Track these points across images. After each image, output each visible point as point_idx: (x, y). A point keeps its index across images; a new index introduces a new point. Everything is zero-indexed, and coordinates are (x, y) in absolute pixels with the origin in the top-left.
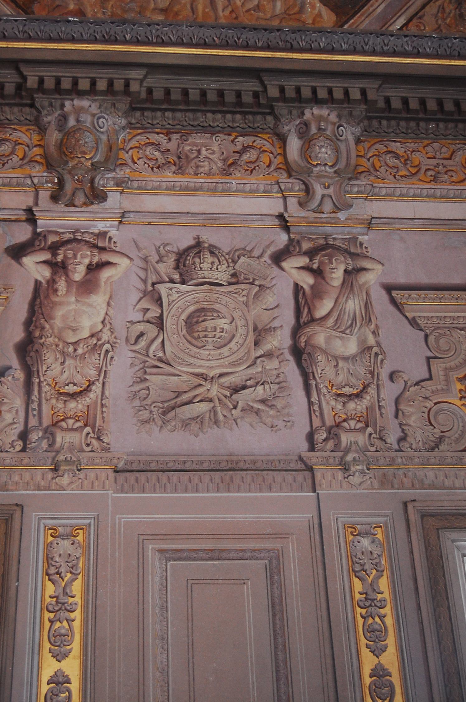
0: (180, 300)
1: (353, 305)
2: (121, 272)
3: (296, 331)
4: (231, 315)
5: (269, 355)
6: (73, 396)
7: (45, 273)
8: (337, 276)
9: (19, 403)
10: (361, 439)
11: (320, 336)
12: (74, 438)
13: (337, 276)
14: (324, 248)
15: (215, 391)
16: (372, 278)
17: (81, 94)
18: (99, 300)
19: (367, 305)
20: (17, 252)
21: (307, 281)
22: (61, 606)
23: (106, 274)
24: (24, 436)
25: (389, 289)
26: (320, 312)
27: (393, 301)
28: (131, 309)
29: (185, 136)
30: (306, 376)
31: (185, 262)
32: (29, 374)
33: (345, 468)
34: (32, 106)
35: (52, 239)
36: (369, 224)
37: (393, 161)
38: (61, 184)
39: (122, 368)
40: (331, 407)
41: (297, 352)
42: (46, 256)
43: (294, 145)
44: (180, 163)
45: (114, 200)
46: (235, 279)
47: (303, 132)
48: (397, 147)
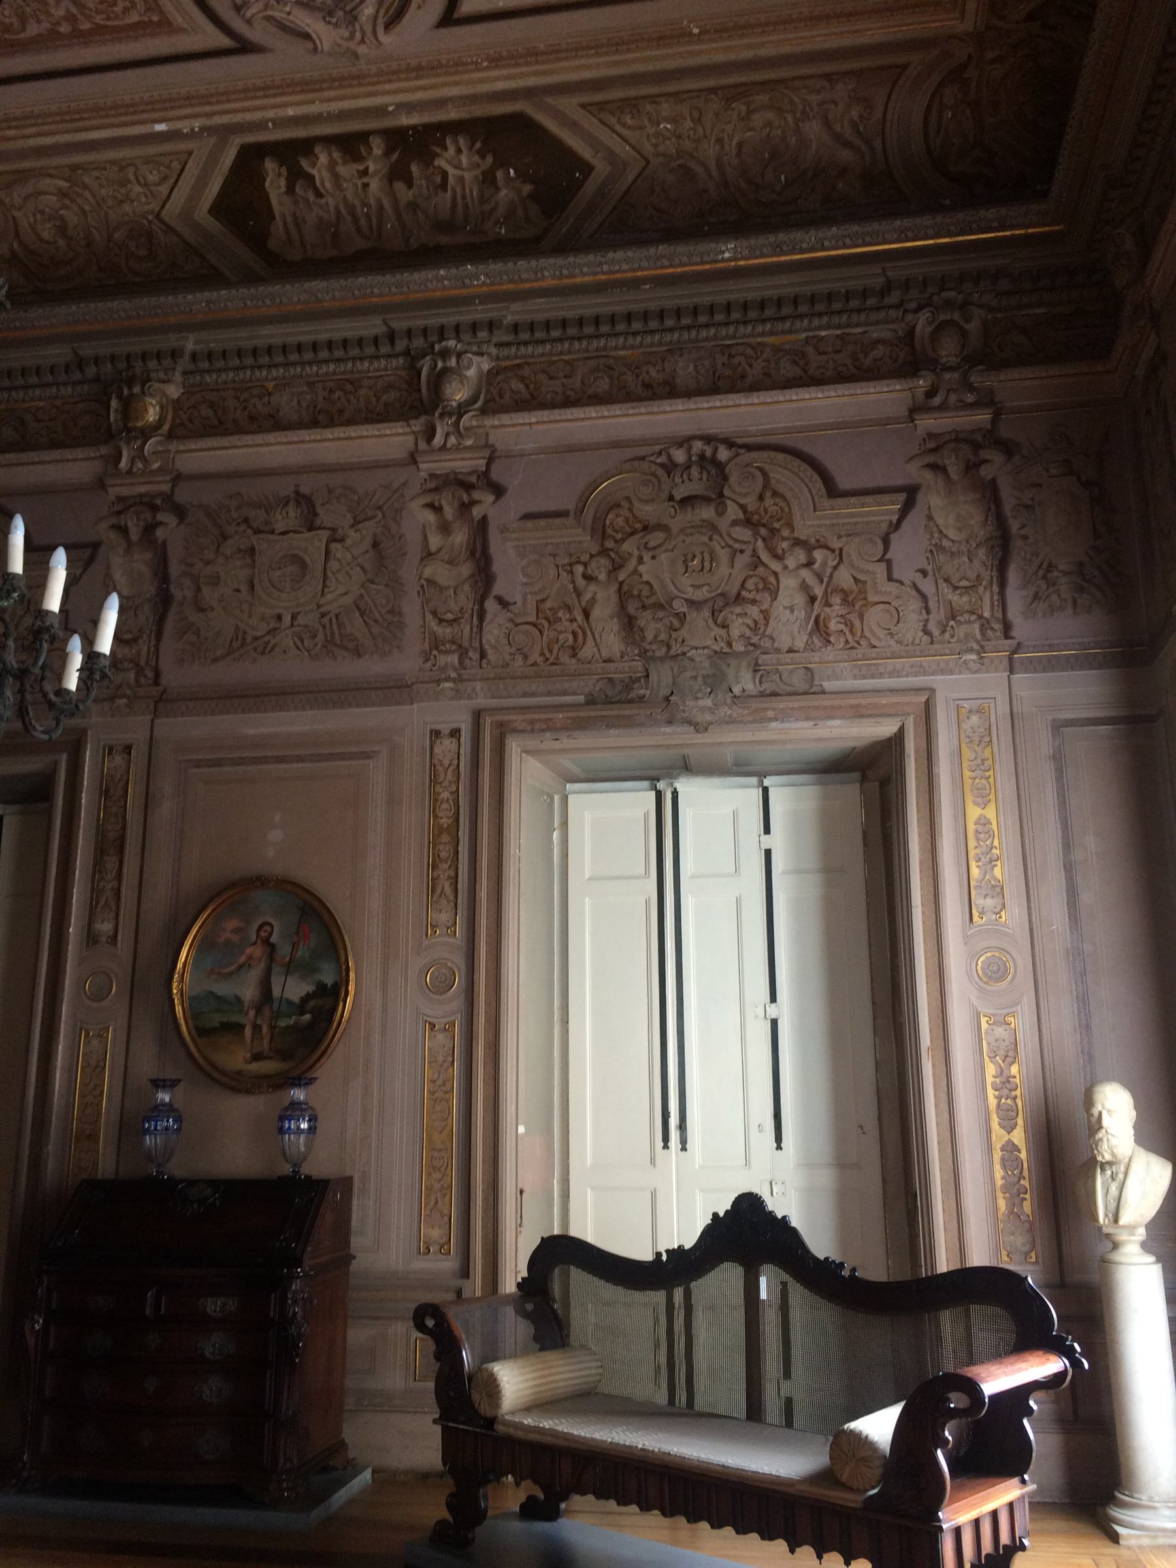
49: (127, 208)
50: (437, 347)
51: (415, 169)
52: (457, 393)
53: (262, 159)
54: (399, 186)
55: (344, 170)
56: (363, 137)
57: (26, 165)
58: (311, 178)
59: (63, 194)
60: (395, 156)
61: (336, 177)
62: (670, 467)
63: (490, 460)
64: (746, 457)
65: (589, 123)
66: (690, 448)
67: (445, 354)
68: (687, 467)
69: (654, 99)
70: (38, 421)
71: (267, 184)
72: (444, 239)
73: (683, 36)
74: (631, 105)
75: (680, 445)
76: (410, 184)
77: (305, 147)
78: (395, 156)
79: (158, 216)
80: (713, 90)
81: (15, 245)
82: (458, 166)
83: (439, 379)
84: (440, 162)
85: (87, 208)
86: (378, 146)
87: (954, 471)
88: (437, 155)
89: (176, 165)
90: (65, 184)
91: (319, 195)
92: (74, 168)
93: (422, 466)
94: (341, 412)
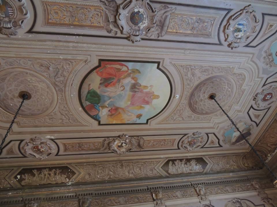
49: (150, 167)
50: (198, 186)
51: (188, 163)
52: (202, 193)
53: (170, 161)
54: (186, 165)
55: (179, 163)
56: (183, 159)
57: (139, 161)
58: (175, 164)
59: (142, 164)
60: (186, 161)
61: (178, 164)
62: (234, 202)
63: (210, 202)
64: (242, 201)
65: (209, 159)
66: (235, 200)
67: (200, 187)
68: (236, 202)
69: (216, 157)
70: (140, 198)
71: (169, 164)
72: (191, 172)
73: (223, 150)
74: (213, 157)
75: (233, 199)
76: (187, 165)
77: (176, 160)
78: (186, 161)
79: (154, 168)
80: (222, 156)
81: (133, 171)
82: (193, 163)
83: (200, 191)
84: (191, 162)
85: (145, 166)
86: (184, 160)
87: (267, 202)
88: (191, 162)
89: (159, 162)
90: (143, 163)
91: (175, 166)
92: (145, 162)
93: (201, 203)
94: (186, 195)
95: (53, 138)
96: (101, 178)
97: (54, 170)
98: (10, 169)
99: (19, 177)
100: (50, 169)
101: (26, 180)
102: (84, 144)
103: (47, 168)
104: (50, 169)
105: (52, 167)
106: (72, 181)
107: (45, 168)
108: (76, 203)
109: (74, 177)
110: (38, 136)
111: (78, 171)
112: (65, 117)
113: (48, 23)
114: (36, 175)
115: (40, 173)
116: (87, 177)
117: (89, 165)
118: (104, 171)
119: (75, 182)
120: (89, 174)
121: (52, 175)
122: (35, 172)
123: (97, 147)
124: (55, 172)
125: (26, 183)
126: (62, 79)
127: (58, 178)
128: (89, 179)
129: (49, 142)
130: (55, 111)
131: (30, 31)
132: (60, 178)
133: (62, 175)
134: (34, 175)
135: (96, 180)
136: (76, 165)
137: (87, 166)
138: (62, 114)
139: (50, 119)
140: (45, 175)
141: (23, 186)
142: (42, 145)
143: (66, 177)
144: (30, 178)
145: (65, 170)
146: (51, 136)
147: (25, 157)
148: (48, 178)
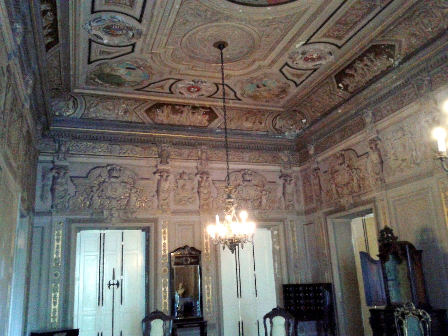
0: (181, 182)
1: (207, 184)
2: (171, 177)
3: (198, 188)
4: (188, 186)
5: (194, 193)
6: (165, 200)
7: (159, 177)
8: (205, 179)
9: (157, 201)
10: (206, 207)
11: (202, 189)
12: (165, 207)
13: (205, 179)
14: (203, 173)
15: (185, 199)
16: (210, 179)
17: (164, 143)
18: (168, 182)
19: (209, 183)
20: (155, 173)
21: (200, 179)
22: (164, 233)
23: (169, 178)
24: (158, 206)
25: (213, 181)
26: (202, 185)
27: (213, 183)
28: (173, 185)
29: (181, 149)
30: (199, 196)
31: (181, 175)
32: (158, 196)
33: (204, 212)
34: (156, 143)
35: (160, 171)
36: (211, 168)
37: (215, 155)
38: (162, 161)
39: (172, 194)
40: (203, 202)
41: (198, 192)
42: (159, 174)
43: (200, 152)
44: (180, 155)
45: (170, 163)
46: (189, 179)
47: (202, 151)
48: (216, 152)
95: (304, 42)
96: (436, 29)
97: (365, 58)
98: (321, 84)
99: (340, 85)
100: (360, 59)
101: (351, 85)
102: (344, 19)
103: (355, 60)
104: (360, 59)
105: (359, 57)
106: (398, 59)
107: (354, 62)
108: (412, 92)
109: (397, 51)
110: (290, 52)
111: (396, 41)
112: (275, 24)
113: (132, 5)
114: (355, 74)
115: (356, 70)
116: (413, 40)
117: (400, 24)
118: (432, 16)
119: (402, 58)
120: (414, 35)
121: (369, 64)
122: (348, 71)
123: (365, 7)
124: (369, 59)
125: (352, 88)
126: (209, 13)
127: (379, 64)
128: (418, 42)
129: (306, 48)
130: (258, 30)
131: (140, 21)
132: (380, 64)
133: (381, 58)
134: (352, 76)
135: (430, 37)
136: (382, 37)
137: (399, 27)
138: (268, 26)
139: (268, 36)
140: (363, 69)
141: (352, 93)
142: (308, 53)
143: (388, 59)
144: (352, 81)
145: (375, 50)
146: (299, 43)
147: (315, 70)
148: (369, 70)
